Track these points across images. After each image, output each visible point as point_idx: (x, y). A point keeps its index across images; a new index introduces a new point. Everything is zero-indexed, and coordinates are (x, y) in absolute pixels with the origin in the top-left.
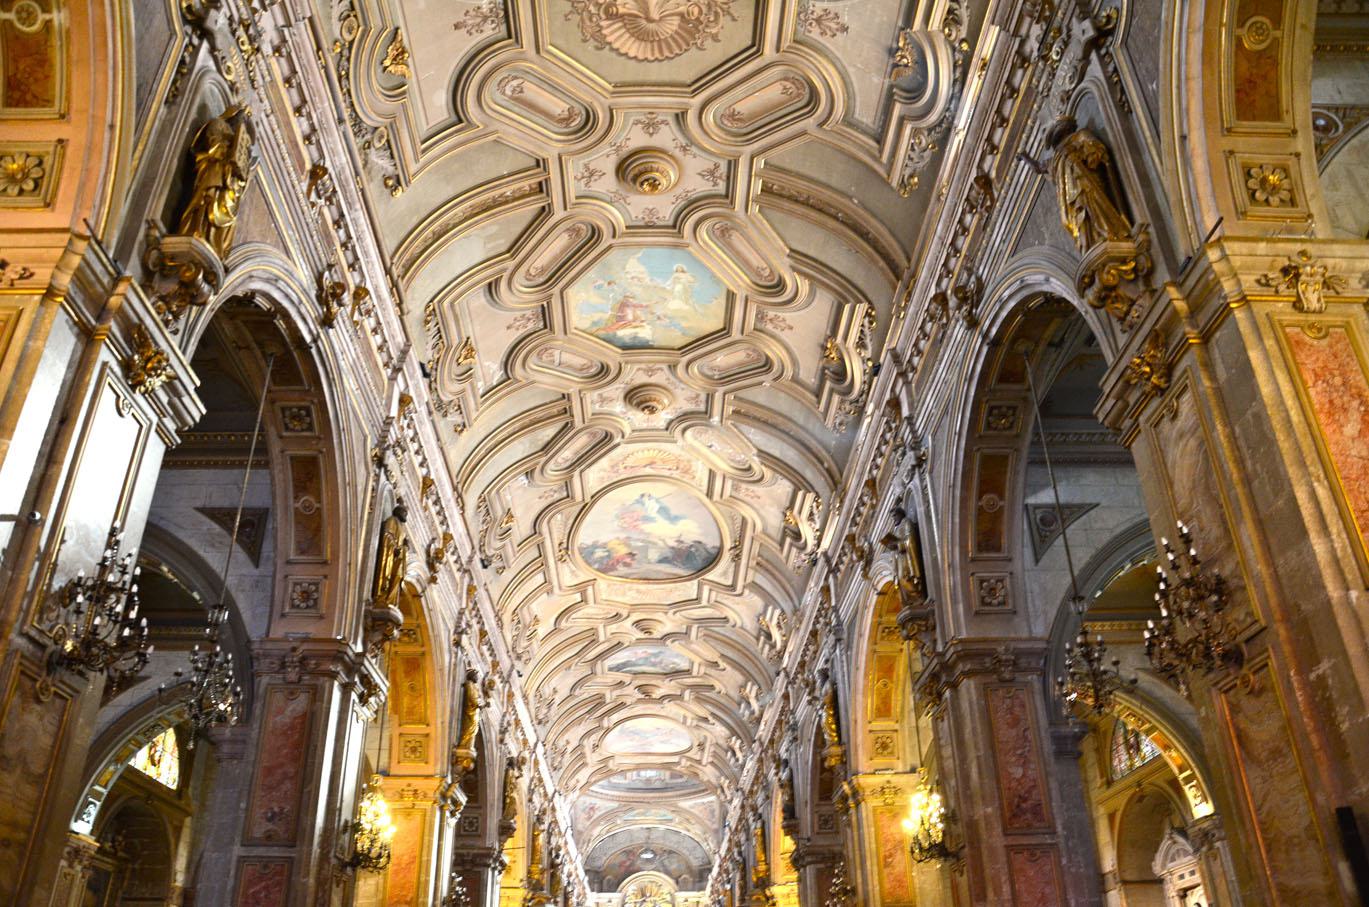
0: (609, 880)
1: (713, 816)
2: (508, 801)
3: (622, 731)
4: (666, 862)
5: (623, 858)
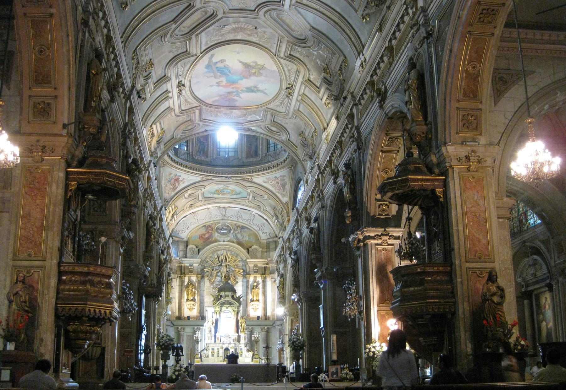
0: (191, 249)
3: (208, 66)
4: (239, 236)
5: (203, 231)
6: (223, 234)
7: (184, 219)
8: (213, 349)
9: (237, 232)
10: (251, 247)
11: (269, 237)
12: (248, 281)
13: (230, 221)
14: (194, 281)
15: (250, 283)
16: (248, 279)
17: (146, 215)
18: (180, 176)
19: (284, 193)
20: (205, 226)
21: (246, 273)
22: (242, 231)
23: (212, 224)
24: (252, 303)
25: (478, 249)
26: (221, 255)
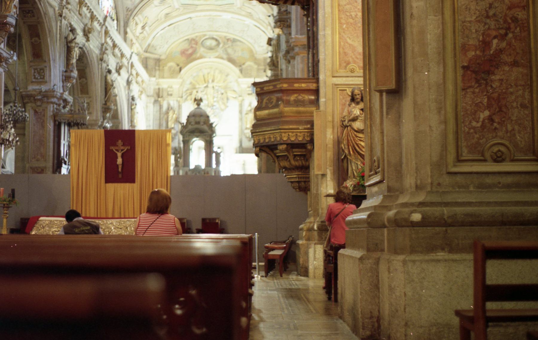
0: (170, 68)
4: (230, 51)
5: (186, 46)
6: (211, 49)
7: (162, 31)
10: (244, 64)
17: (64, 26)
20: (188, 39)
23: (197, 37)
25: (351, 60)
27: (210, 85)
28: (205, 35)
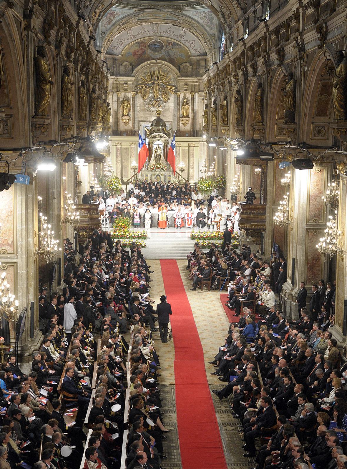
1: (212, 23)
2: (66, 104)
4: (171, 53)
5: (137, 48)
8: (147, 175)
9: (169, 48)
10: (181, 64)
11: (199, 54)
12: (178, 98)
13: (163, 38)
14: (129, 97)
15: (181, 99)
16: (178, 96)
18: (115, 10)
19: (212, 26)
21: (177, 91)
22: (174, 47)
23: (145, 40)
24: (183, 119)
26: (154, 72)
27: (156, 82)
28: (152, 39)
